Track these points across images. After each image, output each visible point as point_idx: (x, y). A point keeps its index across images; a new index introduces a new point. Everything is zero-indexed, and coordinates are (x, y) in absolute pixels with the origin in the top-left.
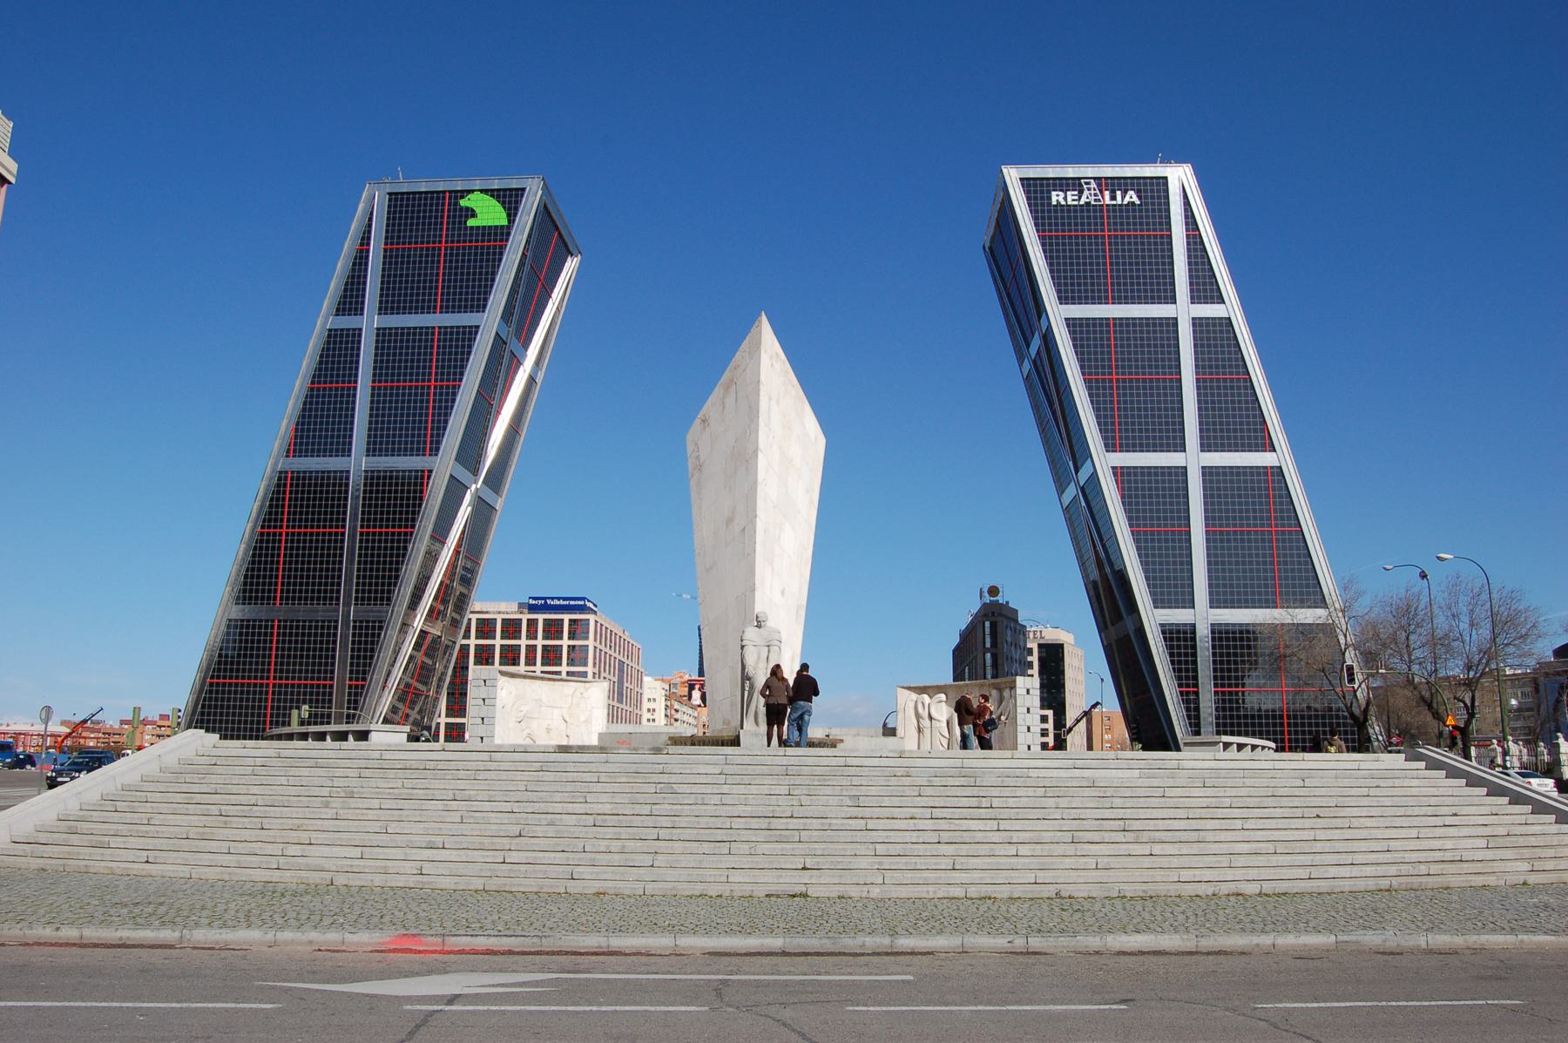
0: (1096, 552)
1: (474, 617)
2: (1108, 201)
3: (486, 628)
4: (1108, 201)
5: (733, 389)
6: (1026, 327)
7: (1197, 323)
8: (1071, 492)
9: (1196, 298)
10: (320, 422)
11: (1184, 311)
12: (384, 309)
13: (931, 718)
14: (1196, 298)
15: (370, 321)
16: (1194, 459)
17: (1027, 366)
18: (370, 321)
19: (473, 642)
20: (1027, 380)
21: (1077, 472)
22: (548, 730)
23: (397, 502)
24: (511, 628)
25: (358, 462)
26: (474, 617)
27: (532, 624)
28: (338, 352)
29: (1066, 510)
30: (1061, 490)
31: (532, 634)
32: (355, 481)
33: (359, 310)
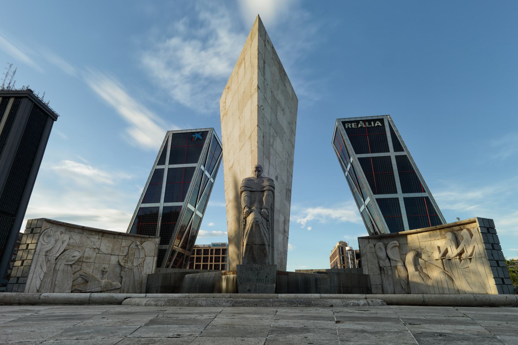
0: (373, 225)
1: (196, 249)
2: (367, 125)
3: (199, 251)
4: (367, 125)
5: (243, 65)
6: (345, 162)
7: (397, 157)
8: (363, 208)
9: (395, 151)
10: (151, 193)
11: (392, 154)
12: (170, 163)
13: (389, 259)
14: (395, 151)
15: (166, 167)
16: (400, 195)
17: (347, 173)
18: (166, 167)
19: (195, 256)
20: (347, 177)
21: (364, 201)
22: (103, 272)
23: (171, 215)
24: (206, 251)
25: (161, 205)
26: (196, 249)
27: (212, 250)
28: (157, 175)
29: (361, 213)
30: (359, 208)
31: (212, 254)
32: (161, 209)
33: (163, 163)
